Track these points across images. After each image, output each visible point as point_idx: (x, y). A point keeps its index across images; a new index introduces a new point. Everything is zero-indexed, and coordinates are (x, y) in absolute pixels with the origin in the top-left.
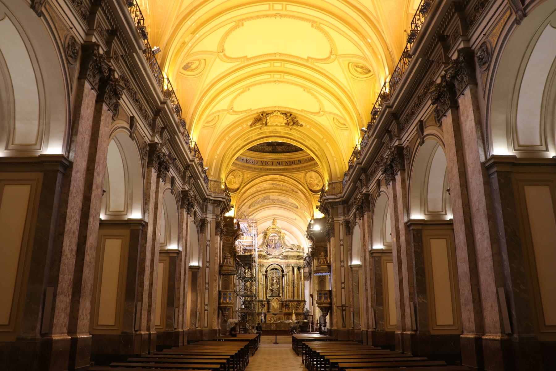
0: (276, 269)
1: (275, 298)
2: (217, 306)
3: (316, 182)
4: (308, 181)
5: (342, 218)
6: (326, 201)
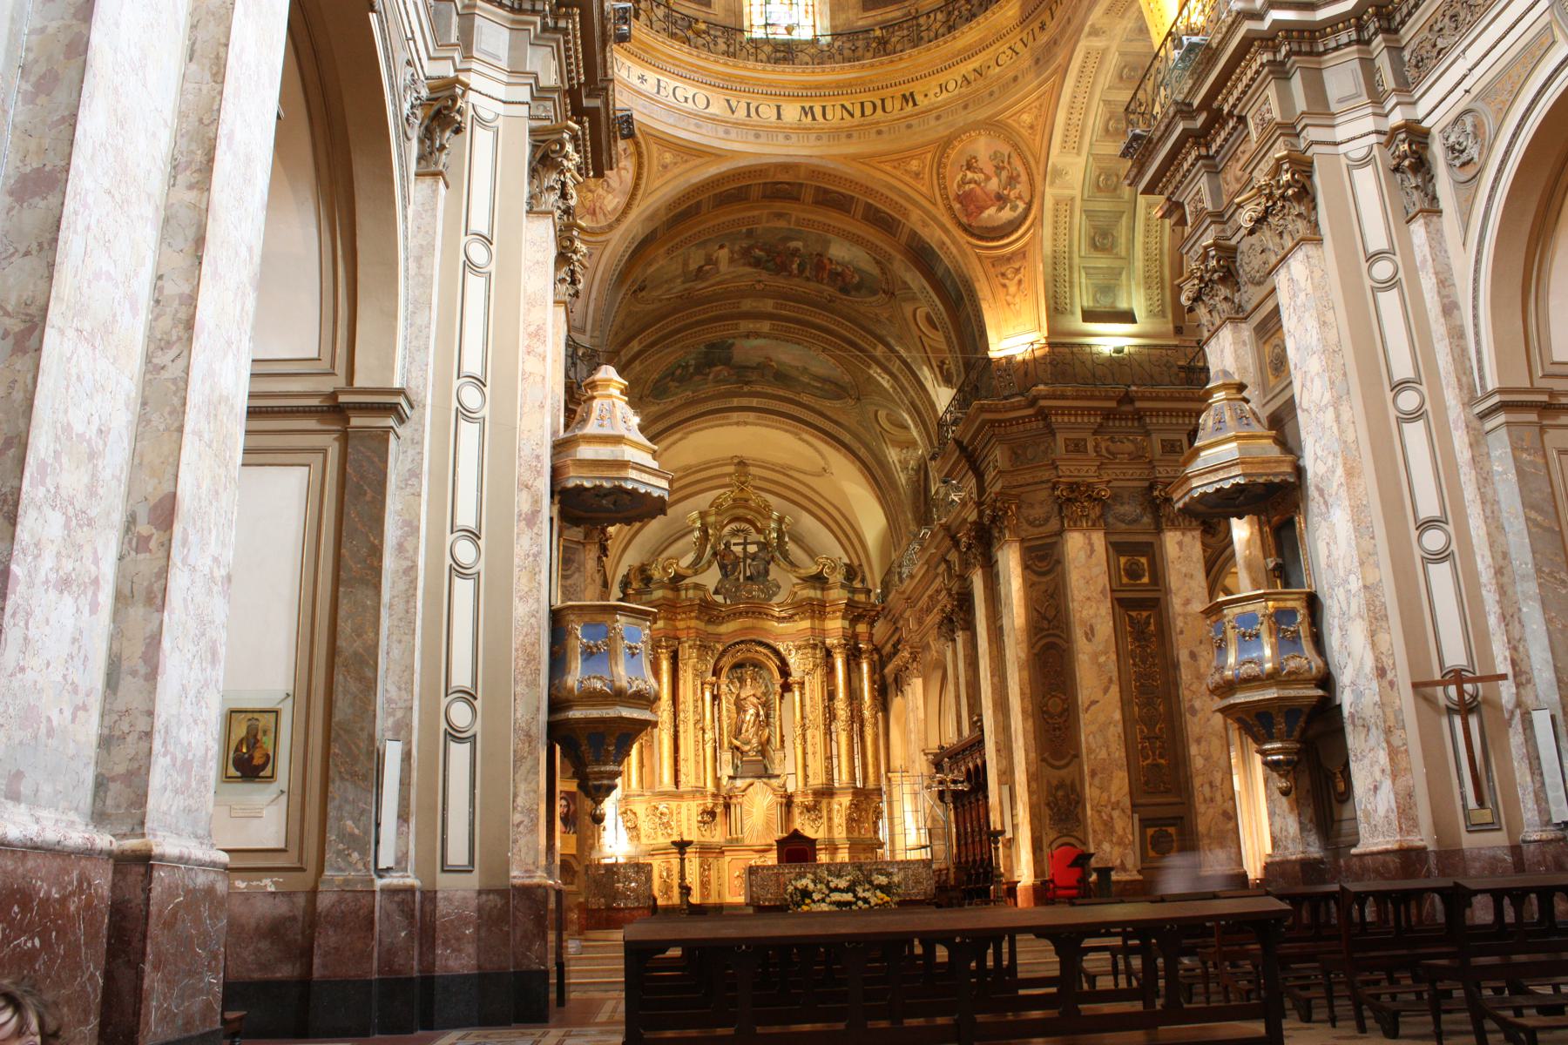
0: (758, 665)
1: (758, 784)
2: (543, 717)
3: (994, 185)
4: (953, 188)
5: (1369, 124)
6: (1248, 25)
